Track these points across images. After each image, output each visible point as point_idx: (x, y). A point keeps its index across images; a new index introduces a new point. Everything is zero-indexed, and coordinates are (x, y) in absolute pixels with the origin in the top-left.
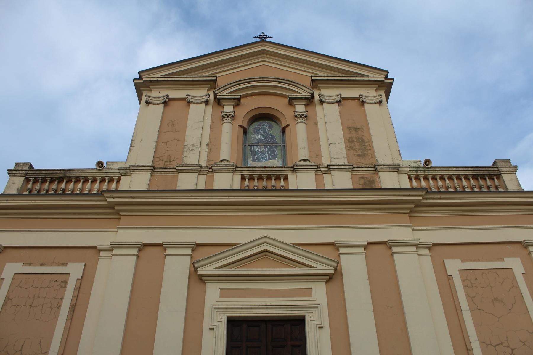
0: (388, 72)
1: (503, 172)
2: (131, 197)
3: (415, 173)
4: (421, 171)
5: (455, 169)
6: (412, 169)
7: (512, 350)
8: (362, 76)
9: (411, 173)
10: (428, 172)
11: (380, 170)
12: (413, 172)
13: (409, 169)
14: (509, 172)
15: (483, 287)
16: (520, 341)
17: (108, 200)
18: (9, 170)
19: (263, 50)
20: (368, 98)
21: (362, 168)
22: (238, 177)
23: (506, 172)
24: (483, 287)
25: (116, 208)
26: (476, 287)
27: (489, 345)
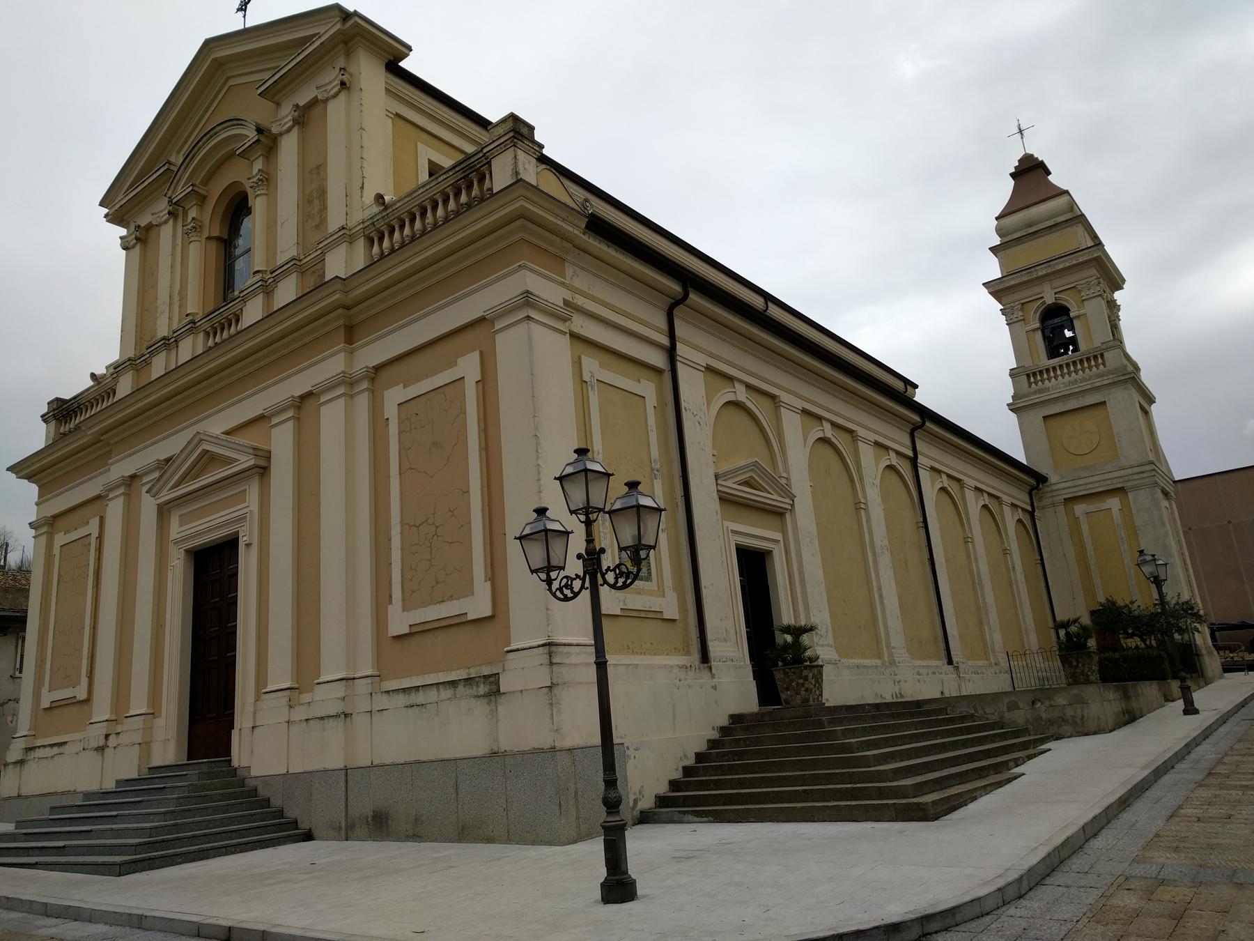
0: (337, 7)
1: (493, 153)
2: (100, 421)
3: (374, 229)
4: (378, 220)
5: (422, 190)
6: (366, 224)
7: (437, 527)
8: (309, 39)
9: (370, 231)
10: (388, 218)
11: (326, 249)
12: (370, 229)
13: (361, 226)
14: (501, 148)
15: (423, 427)
16: (450, 511)
17: (88, 434)
18: (42, 416)
19: (215, 60)
20: (329, 87)
21: (309, 255)
22: (201, 336)
23: (497, 151)
24: (423, 427)
25: (102, 438)
26: (415, 429)
27: (413, 526)
